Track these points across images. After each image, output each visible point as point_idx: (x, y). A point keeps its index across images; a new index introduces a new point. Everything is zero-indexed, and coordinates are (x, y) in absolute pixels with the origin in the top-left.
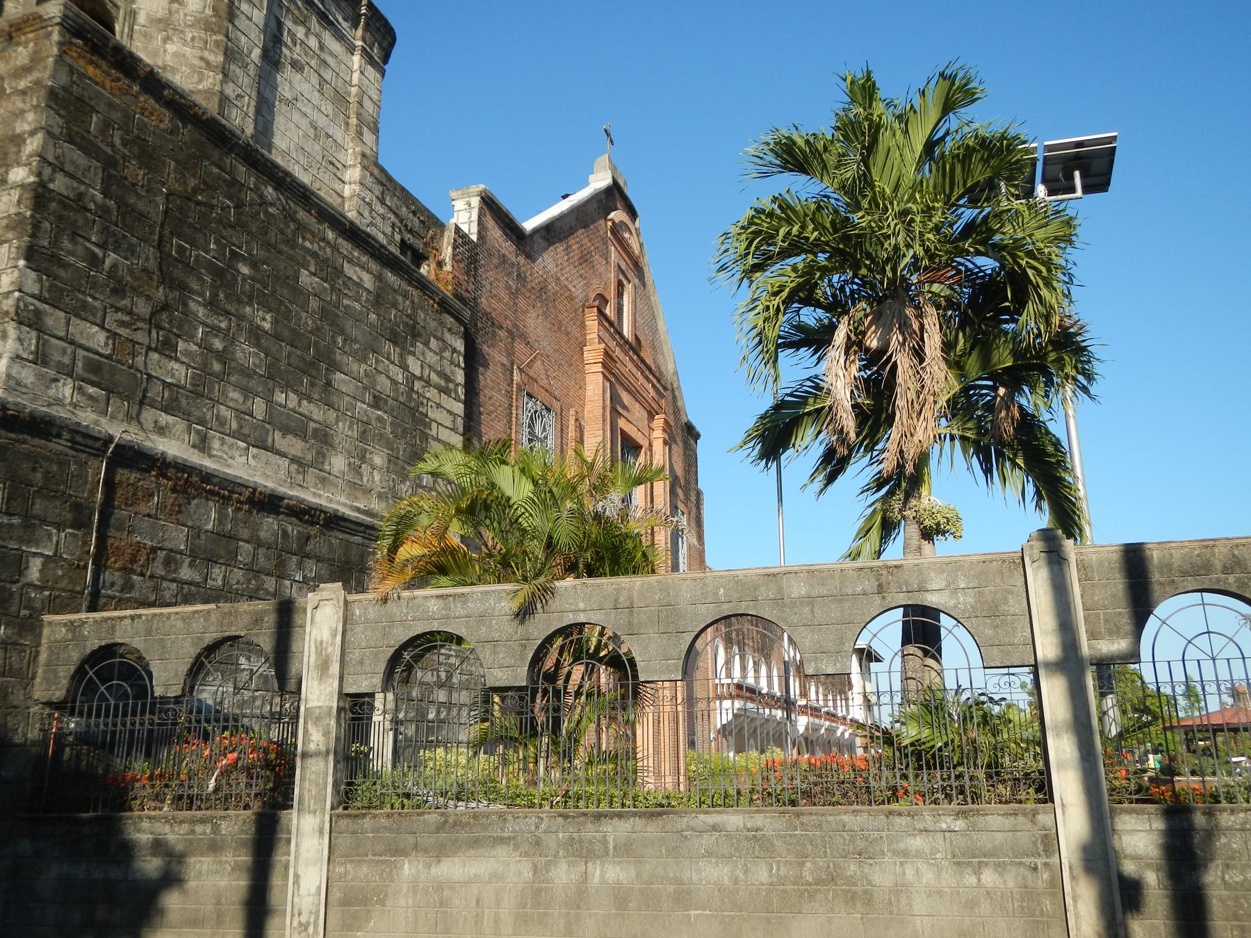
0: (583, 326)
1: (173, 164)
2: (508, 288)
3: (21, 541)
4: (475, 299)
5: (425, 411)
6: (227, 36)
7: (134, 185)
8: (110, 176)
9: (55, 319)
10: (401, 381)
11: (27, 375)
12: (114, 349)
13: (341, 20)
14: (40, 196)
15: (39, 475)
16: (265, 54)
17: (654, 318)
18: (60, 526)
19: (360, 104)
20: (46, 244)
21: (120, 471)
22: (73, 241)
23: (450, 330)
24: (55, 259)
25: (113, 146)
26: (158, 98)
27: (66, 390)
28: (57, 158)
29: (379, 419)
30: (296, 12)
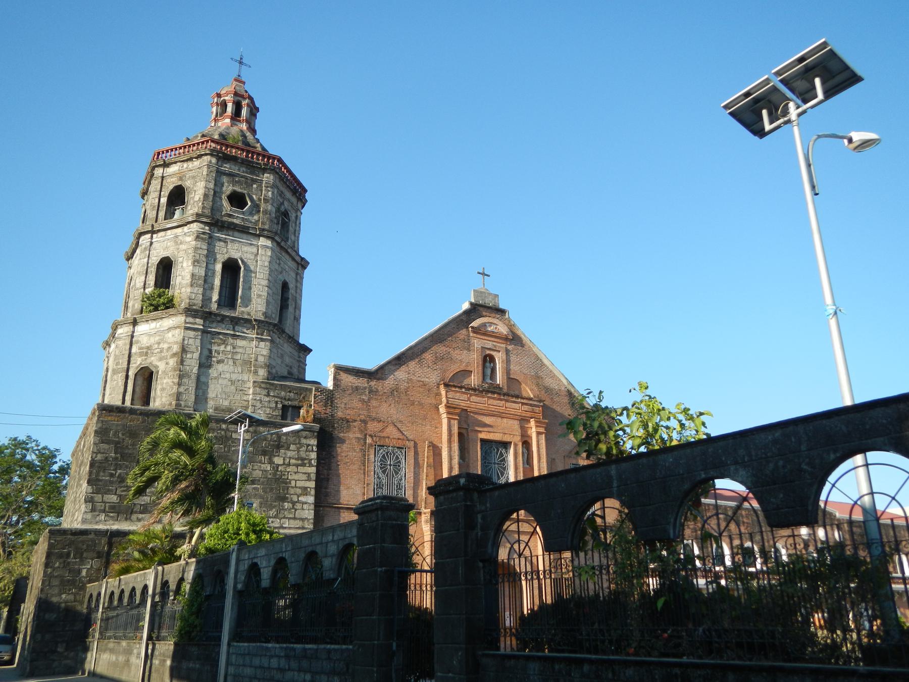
0: (438, 394)
3: (80, 565)
4: (332, 416)
5: (286, 477)
6: (180, 371)
8: (117, 447)
9: (98, 498)
11: (89, 516)
13: (245, 331)
14: (92, 465)
15: (85, 546)
19: (256, 360)
20: (94, 476)
21: (114, 539)
23: (305, 438)
25: (118, 437)
27: (102, 517)
28: (98, 450)
29: (254, 488)
30: (220, 341)
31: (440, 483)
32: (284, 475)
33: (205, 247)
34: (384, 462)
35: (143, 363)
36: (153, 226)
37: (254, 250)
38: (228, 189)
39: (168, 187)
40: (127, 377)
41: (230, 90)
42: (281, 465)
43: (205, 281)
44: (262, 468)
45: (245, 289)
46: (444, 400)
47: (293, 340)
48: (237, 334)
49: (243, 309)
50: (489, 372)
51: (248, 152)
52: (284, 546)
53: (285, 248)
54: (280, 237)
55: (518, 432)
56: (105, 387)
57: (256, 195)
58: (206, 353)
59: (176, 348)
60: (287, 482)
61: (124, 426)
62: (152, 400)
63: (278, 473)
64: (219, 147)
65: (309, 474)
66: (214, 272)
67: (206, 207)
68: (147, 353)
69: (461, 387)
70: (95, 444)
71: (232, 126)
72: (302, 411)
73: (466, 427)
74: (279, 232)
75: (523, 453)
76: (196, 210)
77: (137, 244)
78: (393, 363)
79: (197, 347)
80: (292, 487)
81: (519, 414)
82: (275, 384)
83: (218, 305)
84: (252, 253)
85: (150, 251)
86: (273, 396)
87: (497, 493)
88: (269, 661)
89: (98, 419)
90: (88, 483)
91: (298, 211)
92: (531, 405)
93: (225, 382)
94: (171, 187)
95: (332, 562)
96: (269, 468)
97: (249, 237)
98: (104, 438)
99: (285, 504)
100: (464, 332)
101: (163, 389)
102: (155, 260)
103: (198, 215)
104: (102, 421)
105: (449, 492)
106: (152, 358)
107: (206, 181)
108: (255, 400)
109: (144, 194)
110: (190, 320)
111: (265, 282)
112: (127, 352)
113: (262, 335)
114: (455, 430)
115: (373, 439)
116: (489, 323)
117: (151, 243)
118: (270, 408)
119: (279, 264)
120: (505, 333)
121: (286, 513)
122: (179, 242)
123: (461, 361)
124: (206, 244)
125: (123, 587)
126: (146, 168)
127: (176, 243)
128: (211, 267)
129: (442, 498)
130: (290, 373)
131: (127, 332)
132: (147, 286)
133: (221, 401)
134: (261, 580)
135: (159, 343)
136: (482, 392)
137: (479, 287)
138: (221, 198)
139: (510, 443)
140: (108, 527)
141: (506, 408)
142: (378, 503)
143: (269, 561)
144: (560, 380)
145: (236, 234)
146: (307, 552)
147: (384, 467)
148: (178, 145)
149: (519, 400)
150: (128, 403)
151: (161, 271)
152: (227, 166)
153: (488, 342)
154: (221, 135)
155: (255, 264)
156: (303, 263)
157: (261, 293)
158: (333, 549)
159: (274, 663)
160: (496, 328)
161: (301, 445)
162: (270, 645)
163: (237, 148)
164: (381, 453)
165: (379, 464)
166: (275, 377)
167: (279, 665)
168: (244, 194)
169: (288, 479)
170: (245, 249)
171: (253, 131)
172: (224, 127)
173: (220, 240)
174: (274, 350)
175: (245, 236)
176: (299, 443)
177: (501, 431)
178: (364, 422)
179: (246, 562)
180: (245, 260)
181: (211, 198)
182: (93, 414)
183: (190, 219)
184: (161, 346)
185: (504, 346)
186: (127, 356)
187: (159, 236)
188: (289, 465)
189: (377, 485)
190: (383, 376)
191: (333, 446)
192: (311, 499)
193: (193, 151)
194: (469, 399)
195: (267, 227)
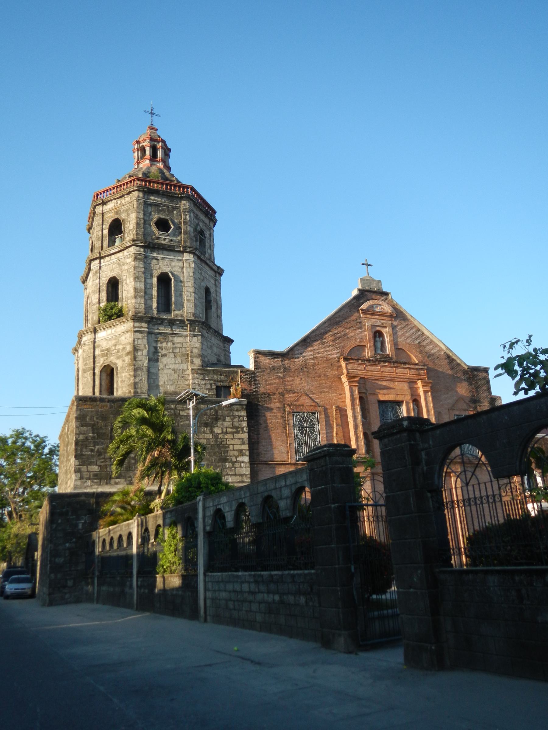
0: (340, 367)
1: (112, 416)
2: (279, 378)
5: (225, 443)
6: (134, 366)
7: (101, 427)
9: (84, 468)
10: (211, 437)
11: (79, 483)
12: (101, 469)
14: (77, 443)
16: (150, 360)
17: (419, 330)
18: (85, 515)
19: (192, 352)
20: (79, 452)
22: (86, 448)
23: (237, 410)
24: (82, 455)
25: (94, 421)
26: (105, 402)
27: (89, 483)
28: (79, 432)
31: (384, 427)
32: (223, 441)
33: (142, 266)
34: (301, 425)
35: (105, 362)
36: (100, 253)
37: (181, 264)
38: (155, 217)
39: (108, 221)
40: (94, 374)
41: (146, 137)
42: (220, 434)
43: (145, 293)
44: (206, 437)
45: (177, 296)
46: (345, 371)
47: (218, 333)
48: (175, 333)
49: (176, 312)
50: (379, 345)
51: (167, 185)
52: (242, 493)
53: (204, 260)
54: (200, 252)
55: (408, 392)
56: (78, 384)
57: (177, 219)
58: (152, 350)
59: (129, 348)
60: (226, 446)
61: (97, 412)
62: (115, 390)
63: (219, 440)
64: (144, 184)
65: (243, 439)
66: (152, 285)
67: (139, 233)
68: (107, 354)
69: (358, 360)
70: (77, 427)
71: (151, 166)
72: (232, 390)
73: (364, 391)
74: (198, 247)
75: (414, 409)
76: (132, 237)
77: (89, 269)
78: (300, 344)
79: (145, 346)
80: (231, 450)
81: (408, 377)
82: (208, 370)
83: (158, 311)
84: (179, 267)
85: (100, 273)
86: (209, 380)
87: (438, 432)
88: (241, 586)
89: (77, 408)
90: (76, 457)
91: (211, 229)
92: (417, 369)
93: (170, 371)
94: (110, 221)
95: (287, 503)
96: (211, 437)
97: (175, 253)
98: (83, 422)
99: (227, 464)
100: (356, 314)
101: (123, 381)
102: (105, 280)
103: (134, 240)
104: (80, 410)
105: (393, 434)
106: (112, 358)
107: (137, 212)
108: (194, 383)
109: (90, 229)
110: (137, 324)
111: (192, 289)
112: (92, 355)
113: (194, 331)
114: (357, 395)
115: (290, 407)
116: (375, 304)
117: (100, 267)
118: (207, 389)
119: (201, 274)
120: (390, 311)
121: (228, 471)
122: (122, 264)
123: (355, 338)
124: (143, 263)
125: (112, 535)
126: (89, 208)
127: (119, 264)
128: (149, 281)
129: (386, 440)
130: (218, 360)
131: (90, 339)
132: (101, 301)
133: (168, 386)
134: (225, 521)
135: (115, 346)
136: (375, 362)
137: (364, 275)
138: (150, 225)
139: (402, 402)
140: (94, 490)
141: (396, 373)
142: (325, 450)
143: (231, 506)
144: (439, 346)
145: (165, 252)
146: (264, 496)
147: (301, 429)
148: (112, 186)
149: (407, 366)
150: (97, 394)
151: (110, 289)
152: (152, 198)
153: (376, 320)
154: (144, 174)
155: (182, 275)
156: (219, 271)
157: (189, 298)
158: (286, 492)
159: (245, 587)
160: (382, 308)
161: (234, 417)
162: (240, 574)
163: (158, 183)
164: (298, 418)
165: (297, 427)
166: (208, 364)
167: (250, 588)
168: (167, 220)
169: (227, 444)
170: (173, 264)
171: (169, 169)
172: (145, 167)
173: (153, 258)
174: (205, 343)
175: (172, 253)
176: (233, 415)
177: (394, 393)
178: (282, 394)
179: (212, 508)
180: (175, 273)
181: (142, 226)
182: (73, 404)
183: (128, 244)
184: (117, 347)
185: (389, 322)
186: (92, 358)
187: (106, 261)
188: (226, 433)
189: (298, 444)
190: (294, 356)
191: (259, 416)
192: (246, 459)
193: (123, 189)
194: (365, 369)
195: (188, 244)
